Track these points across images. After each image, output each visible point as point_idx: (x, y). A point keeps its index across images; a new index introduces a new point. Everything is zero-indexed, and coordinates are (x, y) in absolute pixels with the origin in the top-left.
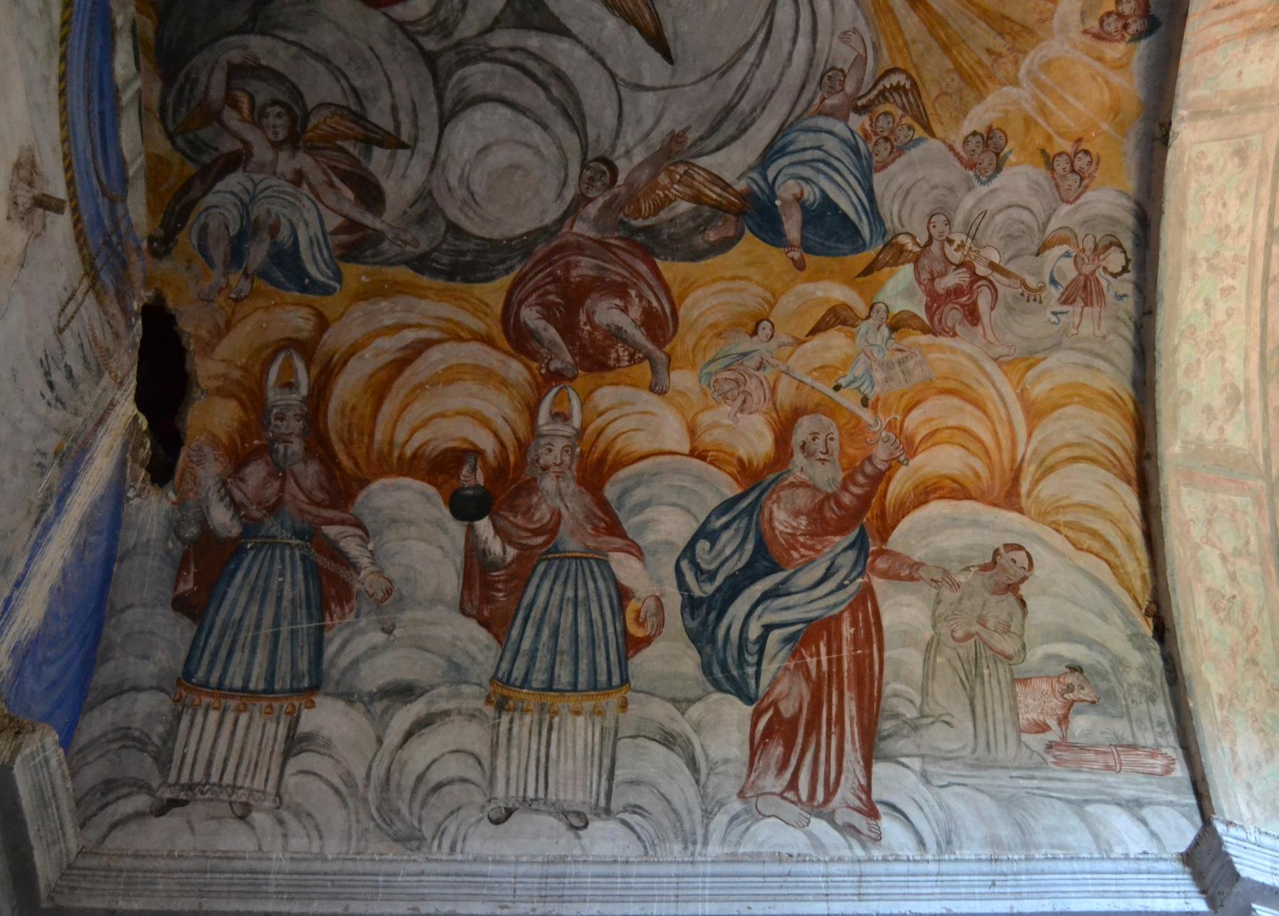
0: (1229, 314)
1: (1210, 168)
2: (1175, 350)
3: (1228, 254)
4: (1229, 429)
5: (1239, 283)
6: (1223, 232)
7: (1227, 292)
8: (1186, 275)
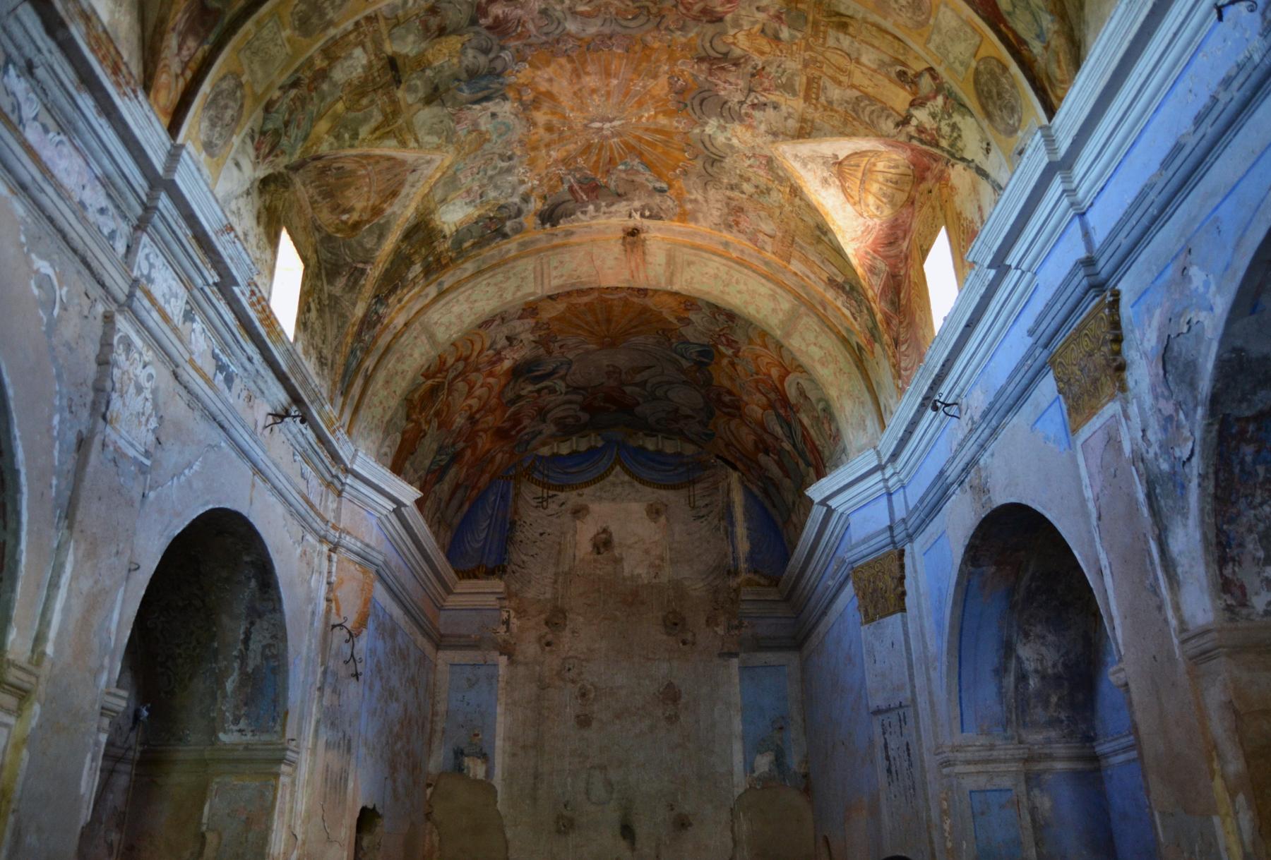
0: (745, 284)
3: (725, 277)
5: (736, 275)
6: (716, 277)
7: (737, 282)
8: (727, 297)
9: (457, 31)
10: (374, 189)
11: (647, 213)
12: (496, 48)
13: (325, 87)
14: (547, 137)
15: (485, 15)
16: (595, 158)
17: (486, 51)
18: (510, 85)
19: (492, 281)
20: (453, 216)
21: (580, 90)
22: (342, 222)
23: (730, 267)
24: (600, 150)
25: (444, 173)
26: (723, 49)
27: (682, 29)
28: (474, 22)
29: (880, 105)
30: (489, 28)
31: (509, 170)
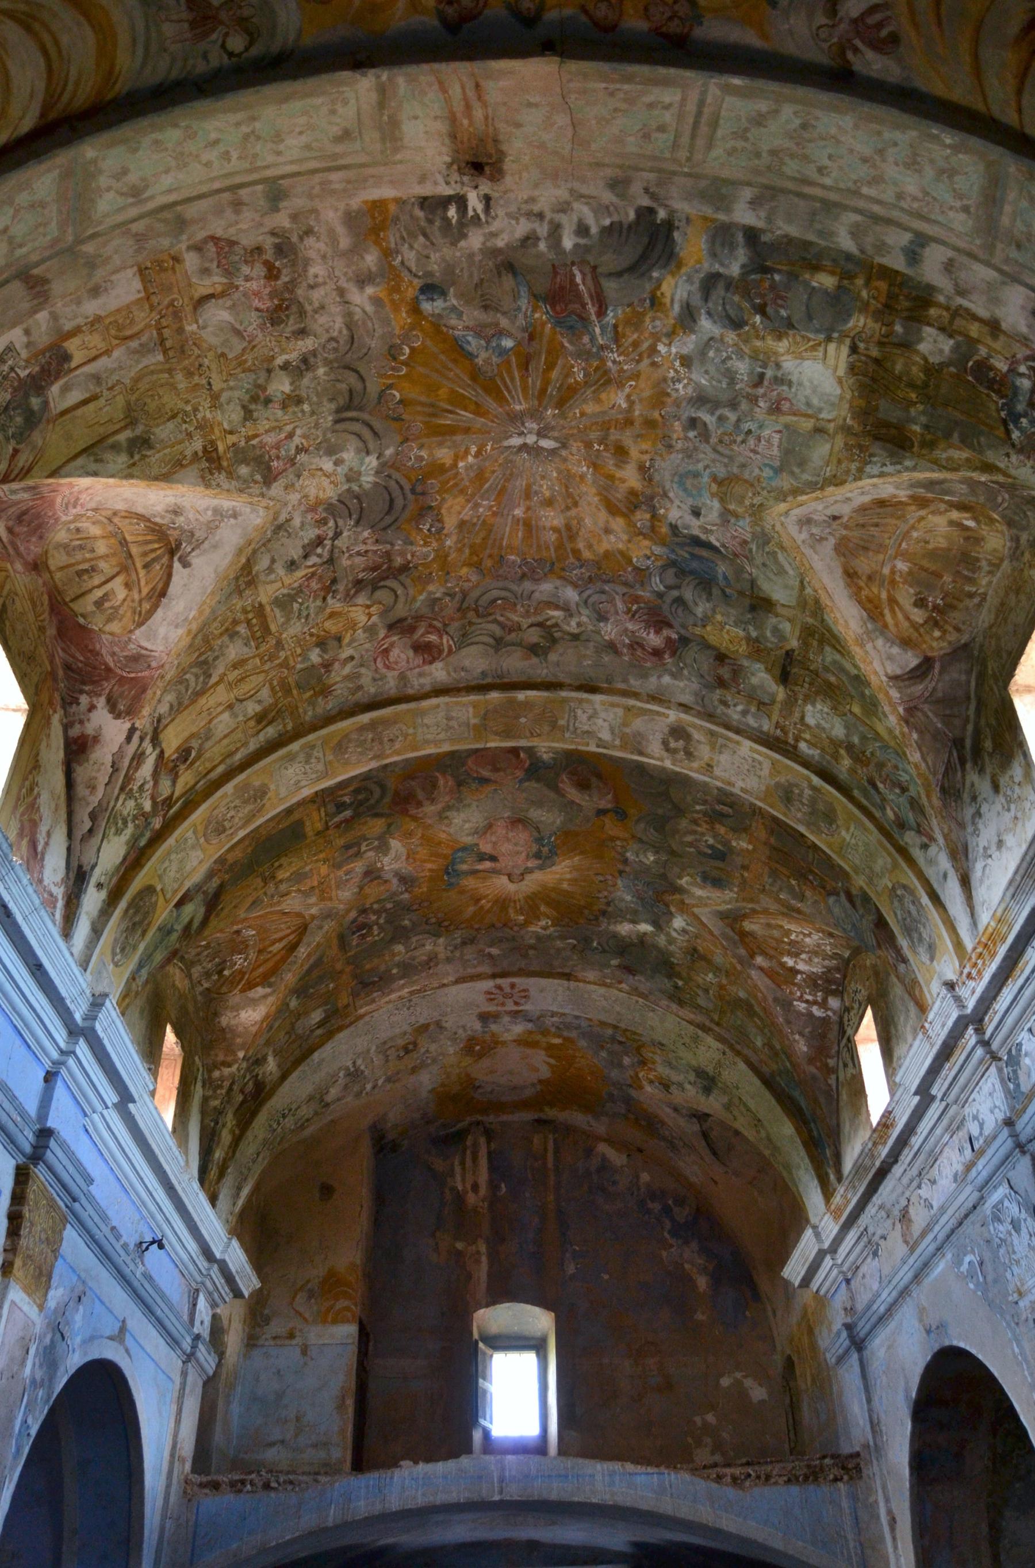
0: (208, 164)
1: (333, 112)
2: (176, 126)
4: (110, 196)
5: (235, 164)
6: (278, 137)
7: (226, 156)
8: (240, 116)
9: (706, 645)
10: (904, 527)
11: (452, 212)
12: (668, 600)
13: (856, 740)
14: (628, 441)
15: (669, 640)
16: (554, 374)
17: (680, 601)
18: (664, 545)
19: (811, 172)
20: (818, 374)
21: (568, 508)
22: (978, 522)
23: (256, 169)
24: (543, 391)
25: (796, 492)
26: (379, 594)
27: (434, 602)
28: (684, 641)
29: (186, 702)
30: (670, 626)
31: (701, 399)
